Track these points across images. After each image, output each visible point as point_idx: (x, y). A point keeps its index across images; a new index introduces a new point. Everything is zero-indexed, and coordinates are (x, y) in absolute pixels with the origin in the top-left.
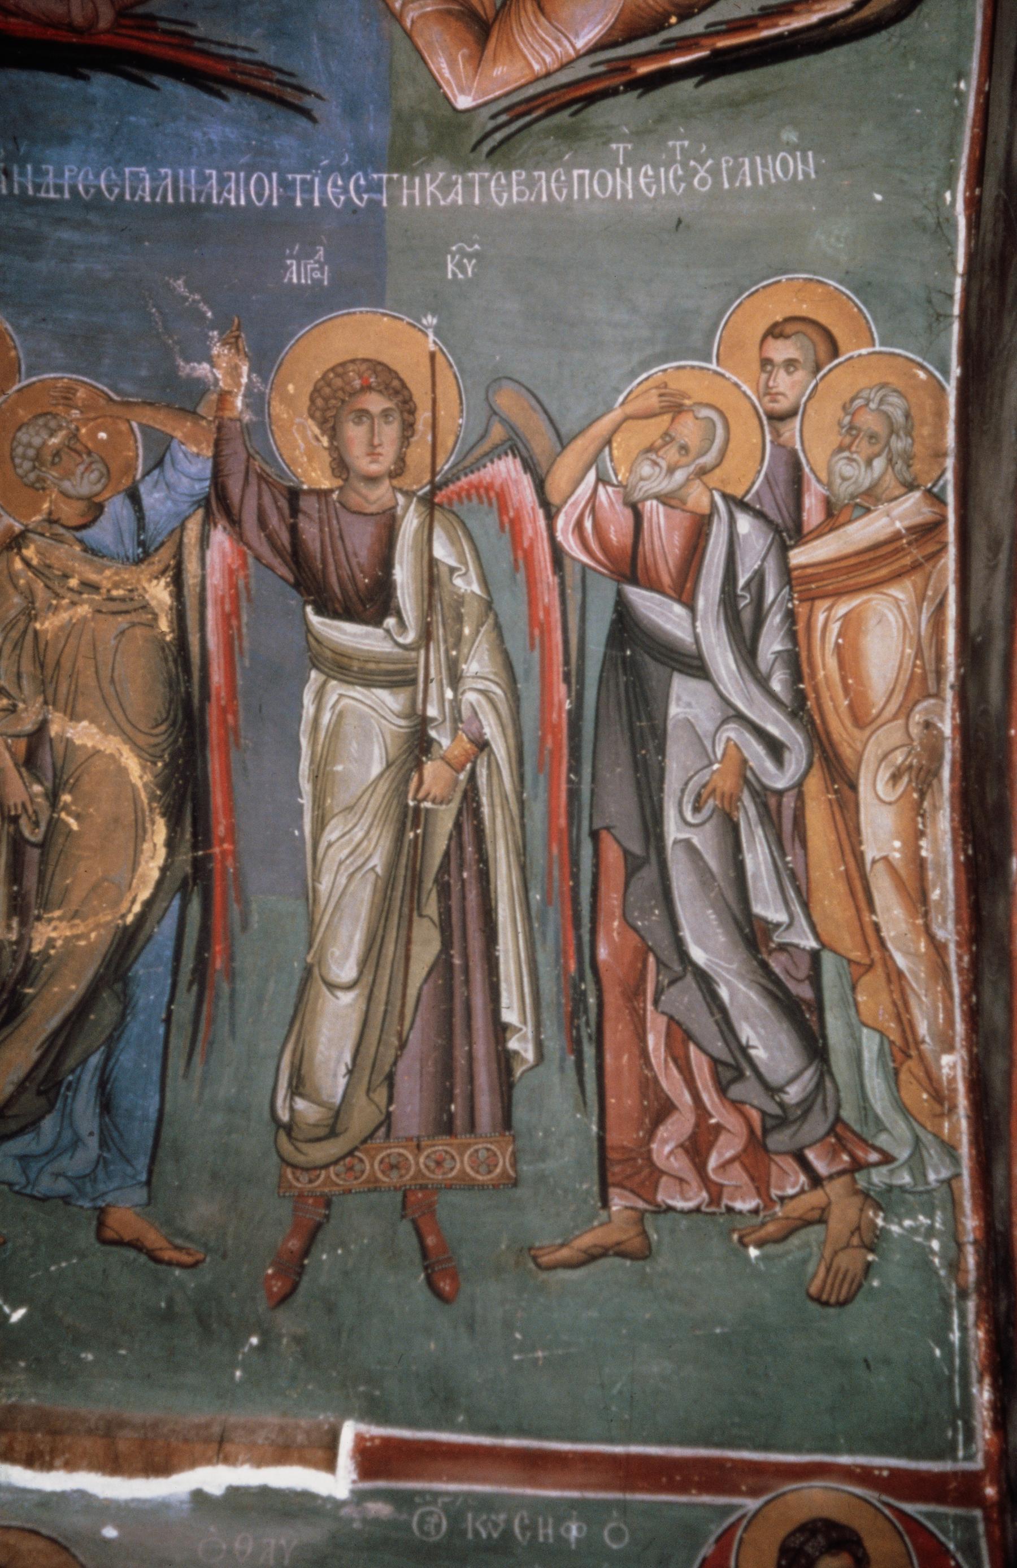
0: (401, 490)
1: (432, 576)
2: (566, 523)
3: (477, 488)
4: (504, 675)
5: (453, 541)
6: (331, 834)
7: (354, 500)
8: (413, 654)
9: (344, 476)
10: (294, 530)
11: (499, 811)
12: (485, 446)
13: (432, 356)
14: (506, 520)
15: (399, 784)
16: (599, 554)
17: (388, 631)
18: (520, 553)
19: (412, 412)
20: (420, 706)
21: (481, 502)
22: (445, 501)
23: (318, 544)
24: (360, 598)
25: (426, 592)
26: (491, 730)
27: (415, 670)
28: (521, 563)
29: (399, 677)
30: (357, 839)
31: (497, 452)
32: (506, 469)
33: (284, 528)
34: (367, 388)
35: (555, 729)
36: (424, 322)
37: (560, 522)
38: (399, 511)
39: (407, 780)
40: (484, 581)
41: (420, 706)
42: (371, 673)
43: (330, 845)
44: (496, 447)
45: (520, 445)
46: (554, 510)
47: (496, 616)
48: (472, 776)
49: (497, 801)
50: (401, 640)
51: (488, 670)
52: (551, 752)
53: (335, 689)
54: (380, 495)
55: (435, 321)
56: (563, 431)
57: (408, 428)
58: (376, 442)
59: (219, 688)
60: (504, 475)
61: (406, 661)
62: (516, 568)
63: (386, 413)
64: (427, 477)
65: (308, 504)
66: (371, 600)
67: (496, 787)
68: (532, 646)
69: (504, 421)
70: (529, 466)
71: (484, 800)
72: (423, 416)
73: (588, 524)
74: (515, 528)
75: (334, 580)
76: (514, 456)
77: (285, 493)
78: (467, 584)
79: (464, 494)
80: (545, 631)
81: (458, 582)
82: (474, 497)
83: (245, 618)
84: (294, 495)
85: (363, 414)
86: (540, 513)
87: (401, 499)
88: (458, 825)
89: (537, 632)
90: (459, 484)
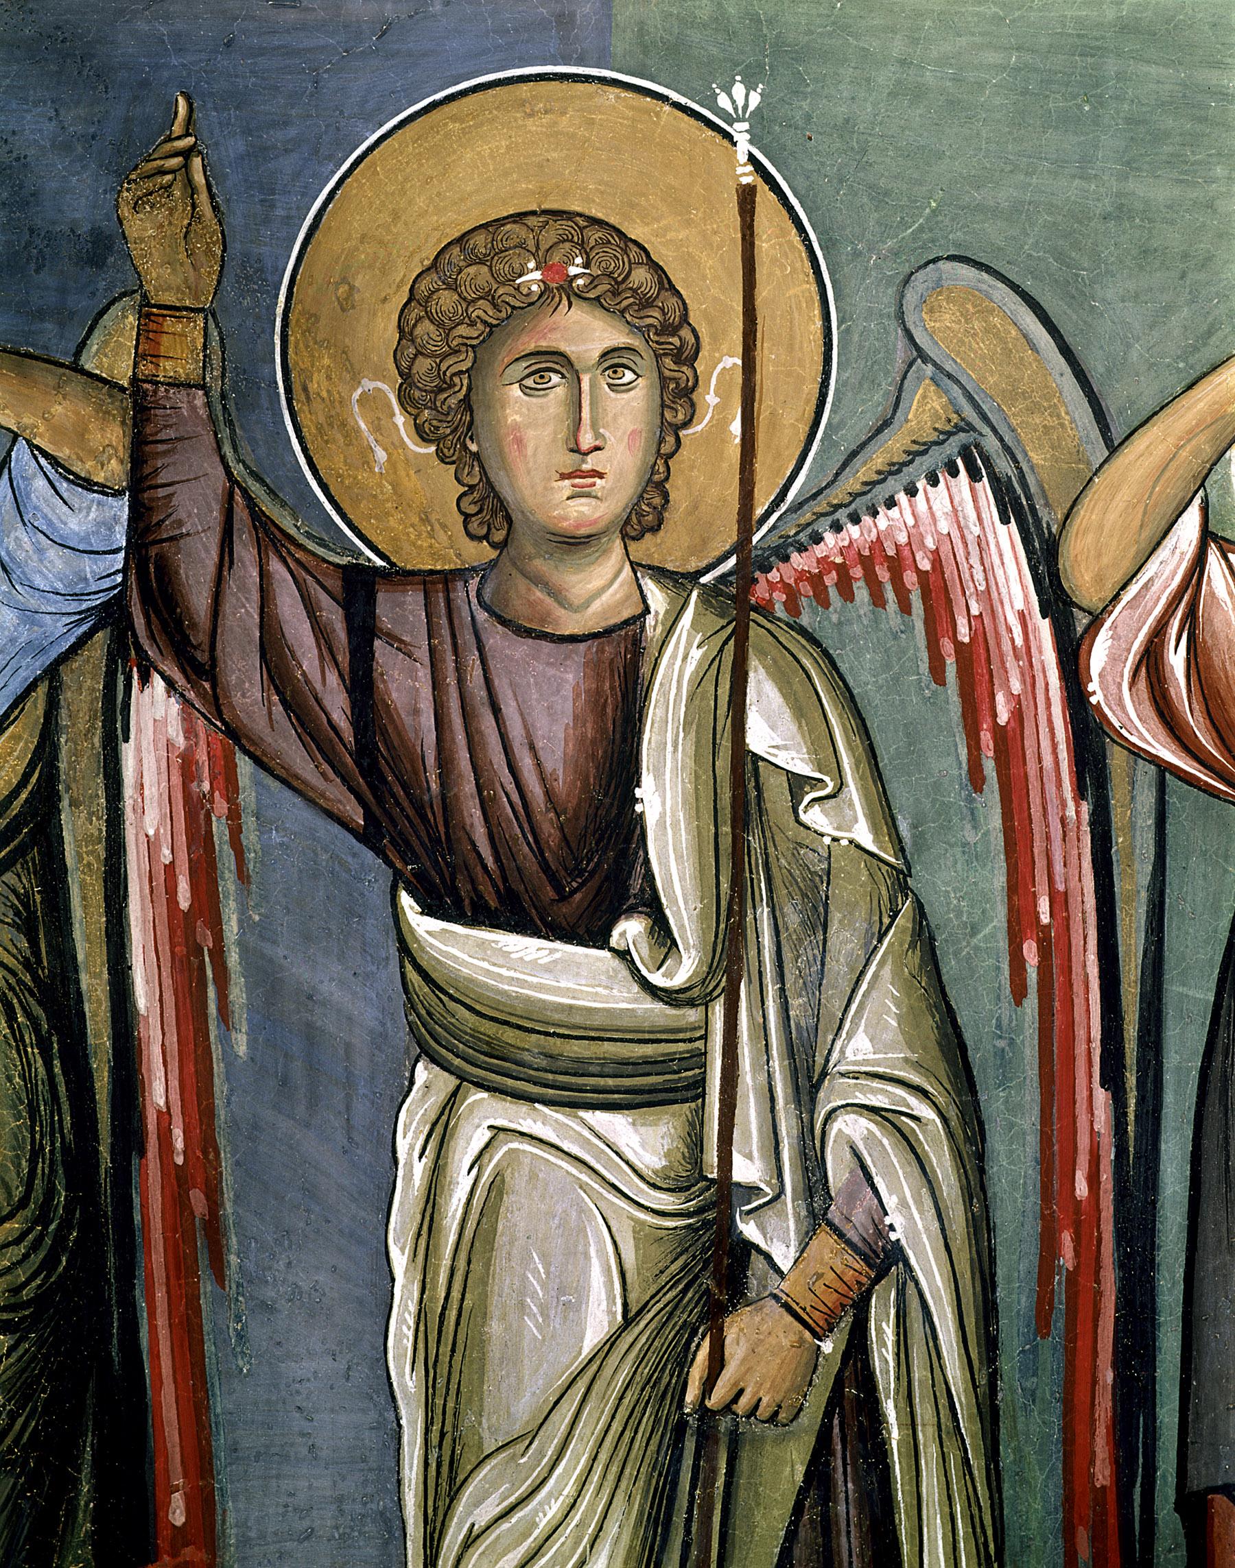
0: (660, 574)
1: (741, 797)
2: (1115, 659)
3: (867, 563)
4: (942, 1069)
5: (803, 708)
6: (476, 1507)
7: (525, 599)
8: (692, 1015)
9: (498, 536)
10: (362, 685)
11: (926, 1436)
12: (894, 445)
13: (747, 197)
14: (947, 647)
15: (659, 1368)
16: (1205, 740)
17: (624, 955)
18: (986, 737)
19: (687, 356)
20: (712, 1156)
21: (878, 600)
22: (779, 597)
23: (428, 720)
24: (545, 866)
25: (726, 842)
26: (909, 1220)
27: (700, 1059)
28: (989, 767)
29: (658, 1077)
30: (544, 1522)
31: (925, 463)
32: (948, 513)
33: (333, 678)
34: (561, 291)
35: (1083, 1220)
36: (723, 101)
37: (1099, 655)
38: (652, 628)
39: (683, 1361)
40: (884, 814)
41: (712, 1156)
42: (580, 1068)
43: (470, 1541)
44: (920, 450)
45: (991, 444)
46: (1082, 621)
47: (919, 907)
48: (858, 1346)
49: (924, 1411)
50: (657, 979)
51: (894, 1060)
52: (1072, 1278)
53: (483, 1113)
54: (599, 590)
55: (755, 100)
56: (1111, 405)
57: (677, 396)
58: (587, 440)
59: (165, 1117)
60: (944, 526)
61: (670, 1034)
62: (976, 779)
63: (613, 360)
64: (730, 537)
65: (401, 611)
66: (576, 872)
67: (919, 1373)
68: (1019, 993)
69: (943, 376)
70: (1011, 503)
71: (890, 1409)
72: (721, 364)
73: (1176, 660)
74: (975, 668)
75: (473, 814)
76: (974, 476)
77: (335, 584)
78: (843, 823)
79: (830, 579)
80: (1055, 947)
81: (815, 817)
82: (862, 593)
83: (231, 928)
84: (360, 587)
85: (557, 361)
86: (1044, 627)
87: (657, 598)
88: (818, 1476)
89: (1030, 951)
90: (819, 551)
